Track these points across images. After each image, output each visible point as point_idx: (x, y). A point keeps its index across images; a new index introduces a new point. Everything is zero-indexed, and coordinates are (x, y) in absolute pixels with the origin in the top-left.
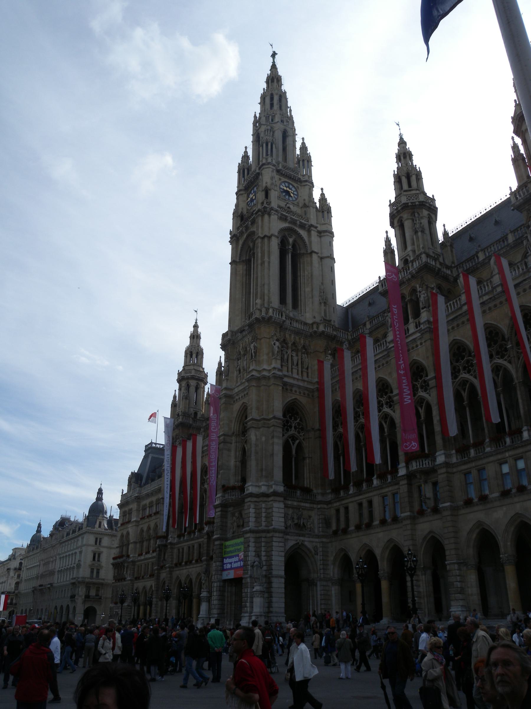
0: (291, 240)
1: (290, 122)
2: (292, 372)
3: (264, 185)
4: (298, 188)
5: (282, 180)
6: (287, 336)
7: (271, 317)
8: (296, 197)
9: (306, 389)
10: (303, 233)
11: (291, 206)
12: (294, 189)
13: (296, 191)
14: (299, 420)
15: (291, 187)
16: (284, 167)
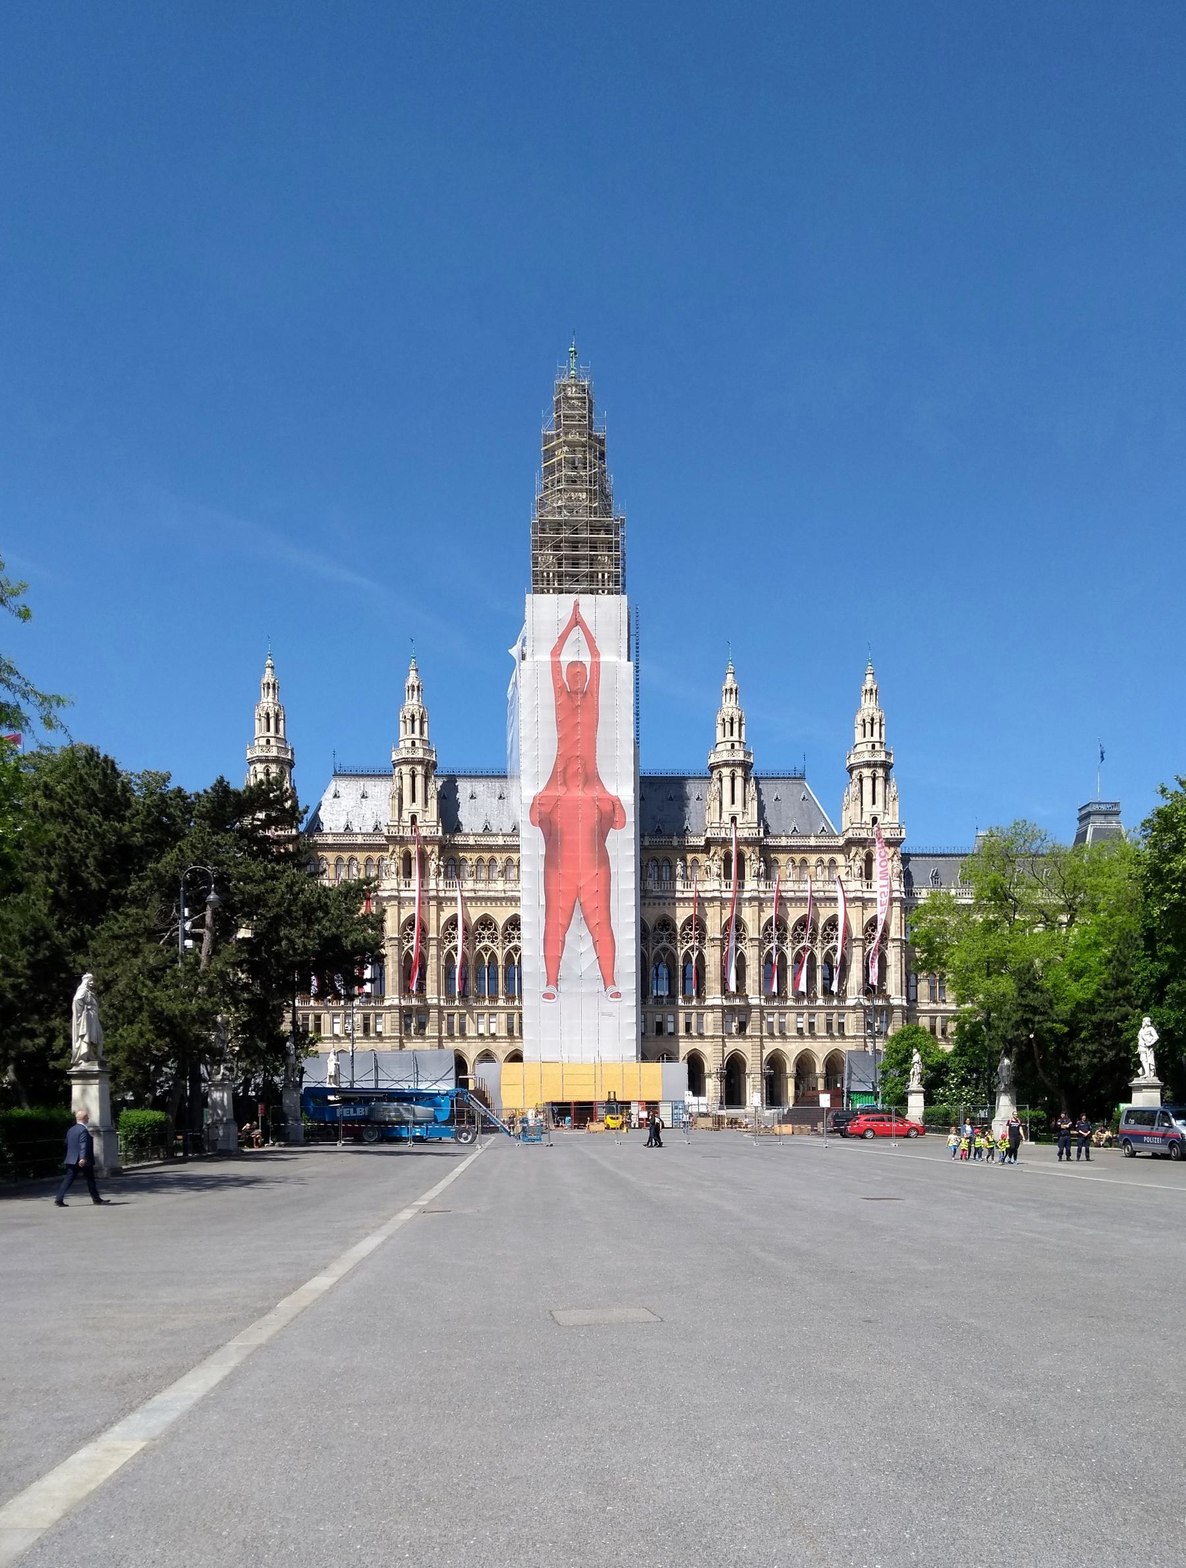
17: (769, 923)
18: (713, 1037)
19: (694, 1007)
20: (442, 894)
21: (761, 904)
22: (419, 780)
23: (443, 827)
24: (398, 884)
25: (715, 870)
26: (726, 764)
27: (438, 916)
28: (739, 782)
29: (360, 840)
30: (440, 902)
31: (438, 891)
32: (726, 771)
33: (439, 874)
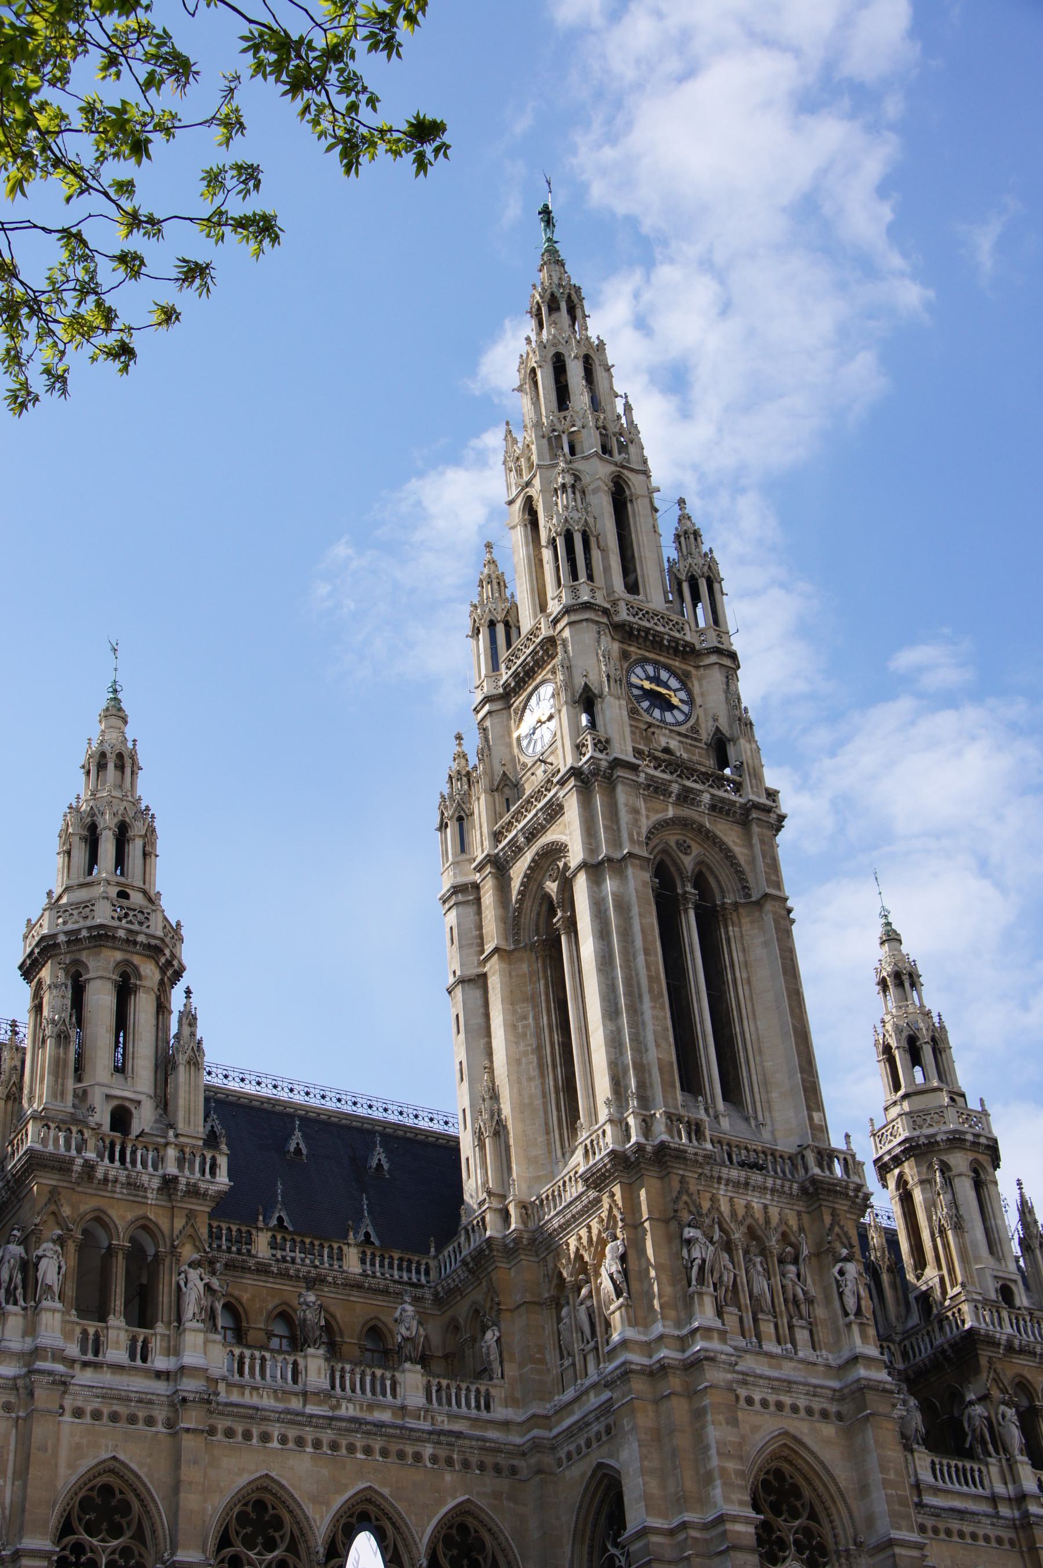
0: (688, 862)
1: (632, 449)
2: (758, 1335)
3: (579, 682)
4: (687, 675)
5: (634, 657)
6: (725, 1208)
7: (663, 1146)
9: (814, 1391)
10: (729, 834)
11: (674, 744)
12: (674, 683)
13: (685, 687)
14: (805, 1515)
15: (664, 675)
16: (635, 611)
26: (956, 1141)
32: (959, 1161)
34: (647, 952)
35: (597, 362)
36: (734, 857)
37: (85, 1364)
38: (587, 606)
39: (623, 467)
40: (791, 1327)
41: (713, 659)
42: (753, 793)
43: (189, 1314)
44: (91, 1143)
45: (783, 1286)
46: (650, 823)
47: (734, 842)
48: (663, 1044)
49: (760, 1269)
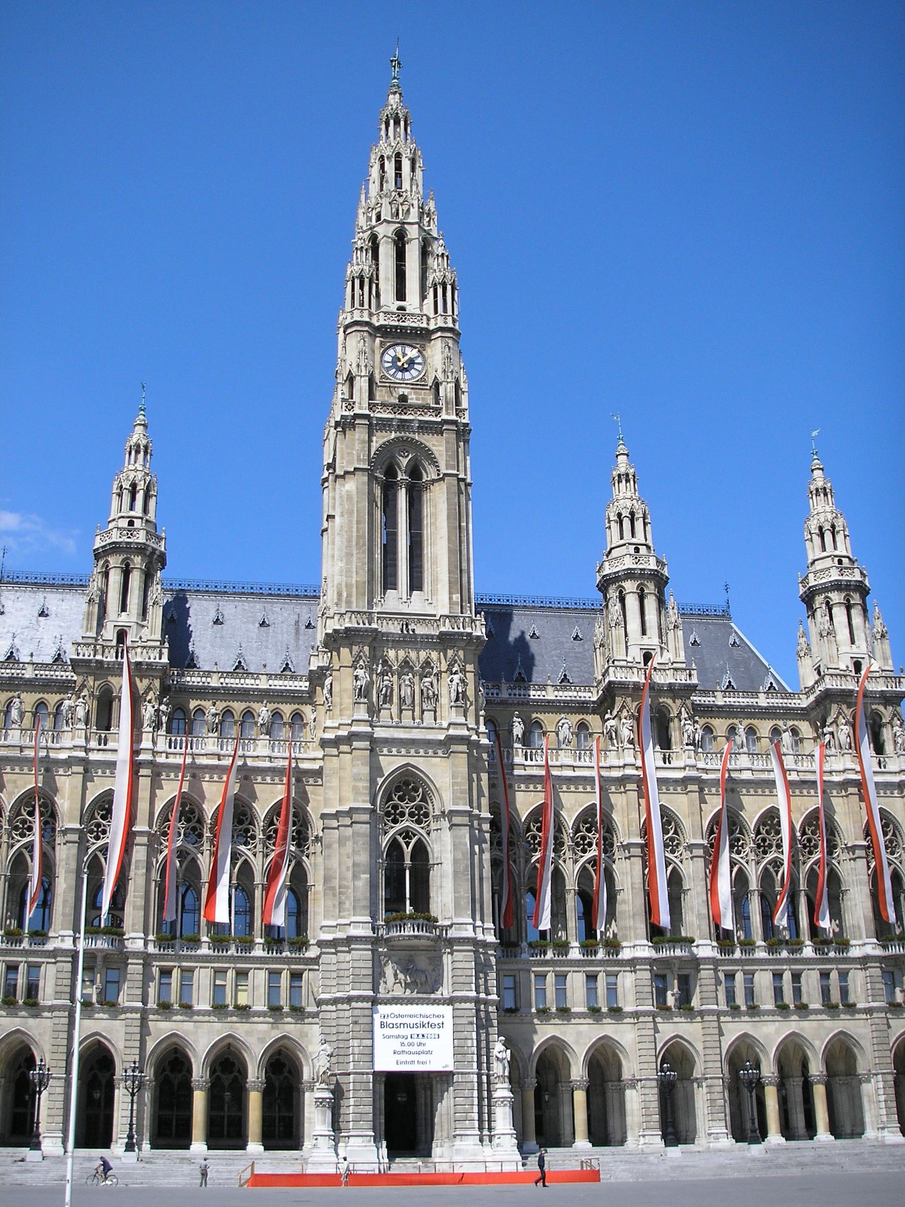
0: (404, 462)
8: (419, 367)
17: (716, 820)
18: (636, 1015)
19: (601, 963)
20: (161, 759)
21: (701, 790)
22: (136, 579)
23: (170, 649)
24: (87, 740)
25: (625, 733)
26: (630, 574)
27: (153, 797)
28: (651, 603)
29: (29, 673)
30: (158, 771)
31: (155, 753)
32: (630, 586)
33: (158, 726)
34: (358, 522)
35: (404, 155)
36: (432, 454)
37: (99, 750)
38: (356, 323)
39: (404, 223)
40: (423, 712)
41: (439, 334)
42: (447, 414)
43: (145, 725)
44: (100, 651)
45: (422, 690)
46: (378, 445)
47: (434, 445)
48: (361, 572)
49: (407, 682)
